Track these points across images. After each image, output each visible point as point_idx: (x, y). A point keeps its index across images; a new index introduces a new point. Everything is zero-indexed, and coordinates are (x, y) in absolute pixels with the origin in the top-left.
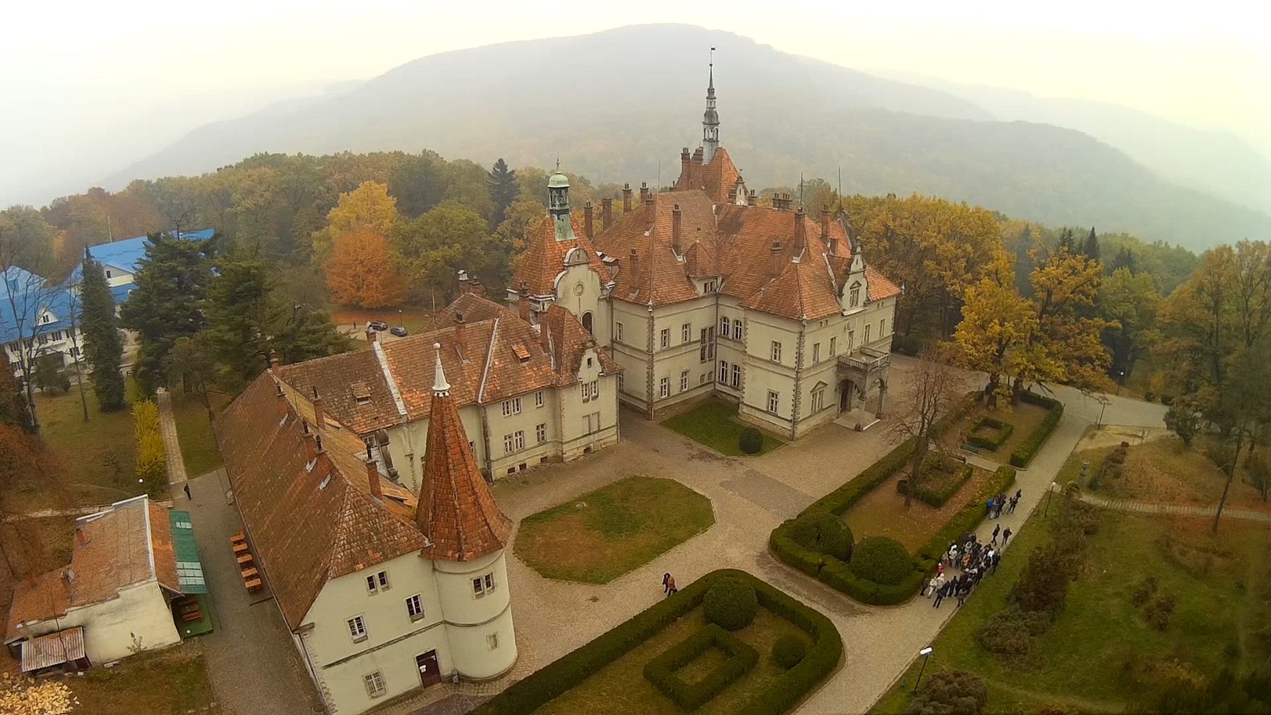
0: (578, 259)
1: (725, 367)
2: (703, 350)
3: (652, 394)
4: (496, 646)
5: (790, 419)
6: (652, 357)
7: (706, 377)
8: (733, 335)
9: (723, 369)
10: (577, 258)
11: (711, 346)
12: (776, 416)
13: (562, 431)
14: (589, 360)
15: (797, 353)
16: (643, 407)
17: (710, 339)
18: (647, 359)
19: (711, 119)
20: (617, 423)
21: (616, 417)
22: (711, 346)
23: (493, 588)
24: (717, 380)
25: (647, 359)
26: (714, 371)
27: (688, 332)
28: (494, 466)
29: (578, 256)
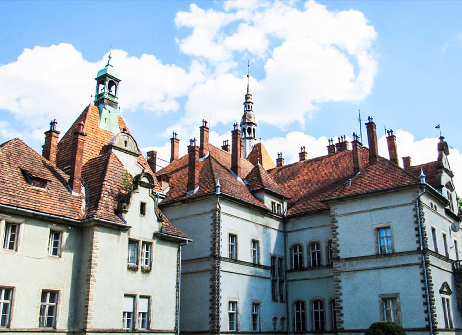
1: (301, 311)
2: (274, 281)
3: (218, 319)
5: (424, 326)
6: (219, 262)
7: (278, 321)
8: (309, 262)
9: (298, 314)
11: (281, 282)
13: (87, 306)
14: (143, 205)
15: (417, 229)
18: (211, 267)
20: (176, 329)
21: (174, 317)
22: (281, 282)
24: (291, 330)
25: (210, 268)
26: (286, 317)
27: (257, 252)
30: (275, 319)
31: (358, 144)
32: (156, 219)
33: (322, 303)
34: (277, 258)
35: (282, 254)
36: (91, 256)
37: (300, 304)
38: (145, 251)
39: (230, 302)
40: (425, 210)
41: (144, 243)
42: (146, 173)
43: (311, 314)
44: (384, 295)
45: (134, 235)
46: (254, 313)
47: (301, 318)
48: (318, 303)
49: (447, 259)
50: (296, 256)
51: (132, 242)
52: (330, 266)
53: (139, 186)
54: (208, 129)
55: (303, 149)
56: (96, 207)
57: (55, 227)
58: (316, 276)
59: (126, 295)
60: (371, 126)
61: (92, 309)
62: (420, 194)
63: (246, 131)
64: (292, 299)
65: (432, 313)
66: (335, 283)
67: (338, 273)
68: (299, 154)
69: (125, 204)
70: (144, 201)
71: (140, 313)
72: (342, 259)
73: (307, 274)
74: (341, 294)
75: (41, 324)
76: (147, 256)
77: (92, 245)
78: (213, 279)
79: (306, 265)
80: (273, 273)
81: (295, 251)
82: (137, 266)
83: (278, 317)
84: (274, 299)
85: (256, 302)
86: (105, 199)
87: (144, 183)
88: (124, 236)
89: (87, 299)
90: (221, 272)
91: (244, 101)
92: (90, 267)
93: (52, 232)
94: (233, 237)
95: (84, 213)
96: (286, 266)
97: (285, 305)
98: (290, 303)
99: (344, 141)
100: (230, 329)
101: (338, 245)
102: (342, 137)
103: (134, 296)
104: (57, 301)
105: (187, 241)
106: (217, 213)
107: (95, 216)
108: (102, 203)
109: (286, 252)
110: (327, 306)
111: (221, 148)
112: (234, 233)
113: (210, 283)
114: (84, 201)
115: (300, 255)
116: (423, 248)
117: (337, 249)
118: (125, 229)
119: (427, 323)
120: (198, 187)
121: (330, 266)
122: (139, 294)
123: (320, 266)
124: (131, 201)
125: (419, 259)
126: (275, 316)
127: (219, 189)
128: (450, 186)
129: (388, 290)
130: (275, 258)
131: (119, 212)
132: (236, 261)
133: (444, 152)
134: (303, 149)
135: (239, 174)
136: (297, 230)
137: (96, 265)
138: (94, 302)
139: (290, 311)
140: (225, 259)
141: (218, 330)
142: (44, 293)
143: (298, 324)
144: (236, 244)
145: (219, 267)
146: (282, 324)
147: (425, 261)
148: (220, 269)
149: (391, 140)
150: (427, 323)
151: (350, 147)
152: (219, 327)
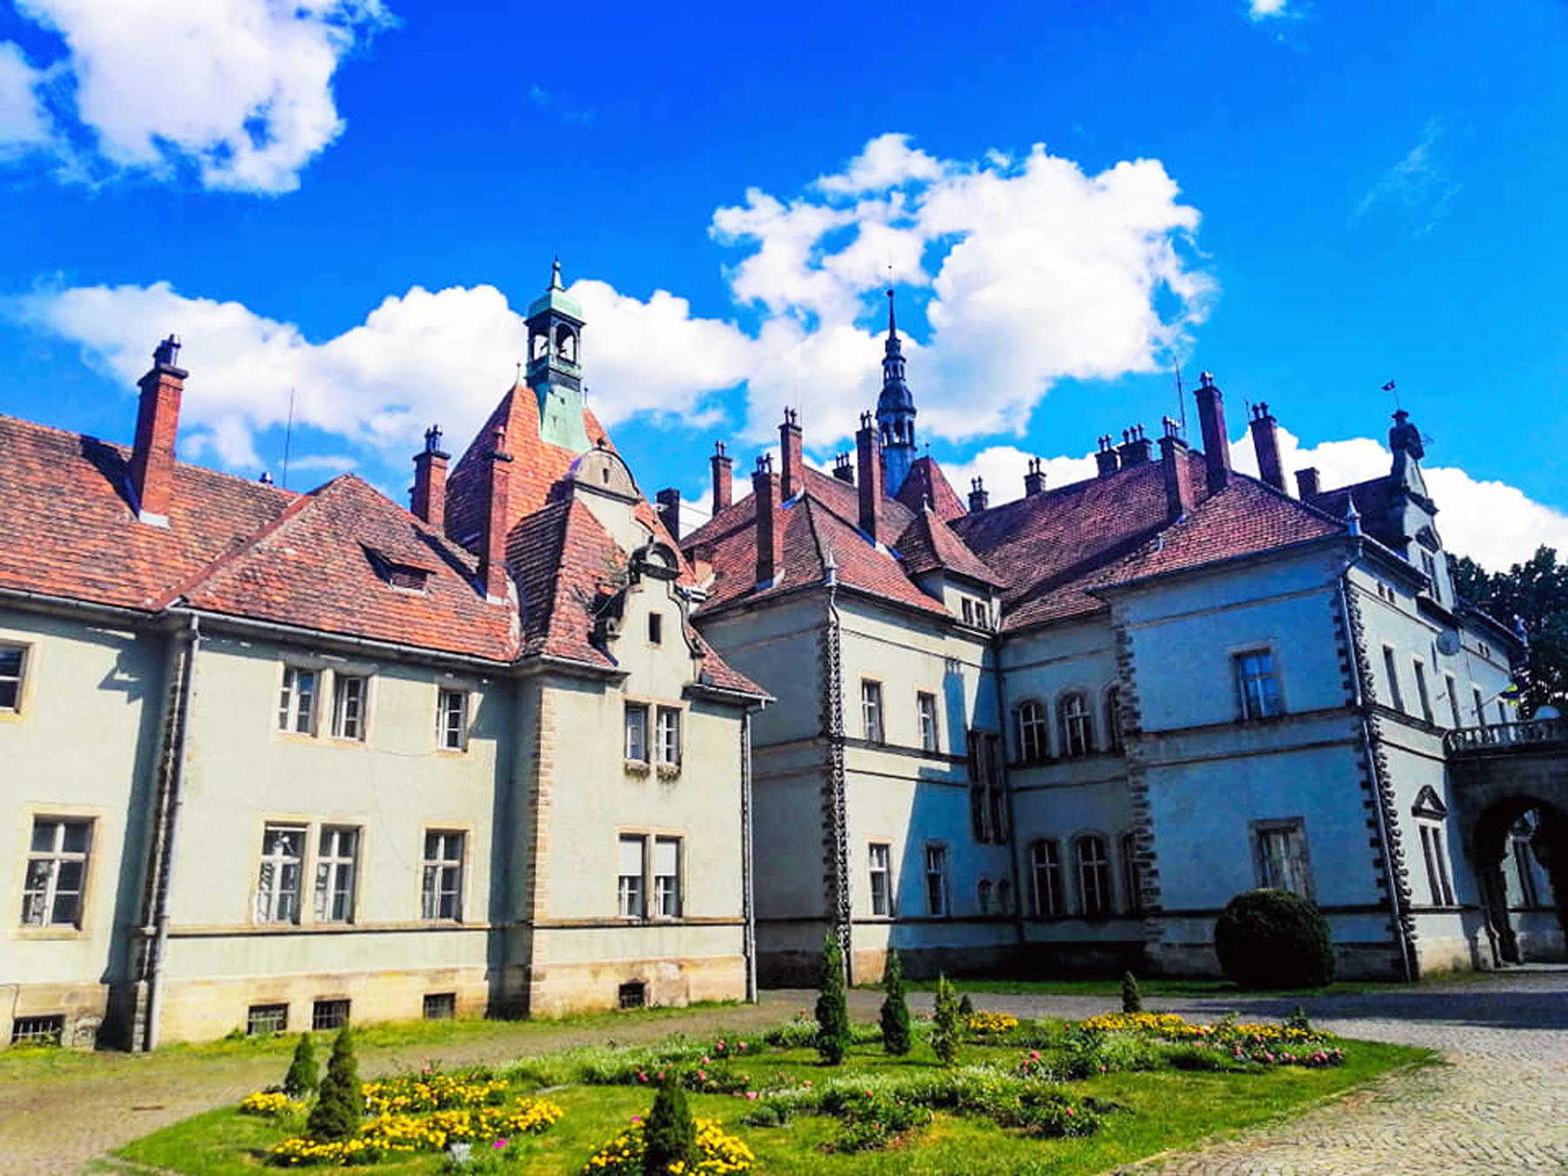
0: (606, 481)
1: (1048, 864)
2: (976, 793)
5: (1375, 900)
7: (993, 890)
8: (1063, 743)
9: (1042, 872)
10: (602, 477)
11: (995, 795)
14: (655, 621)
24: (1026, 910)
26: (1011, 879)
28: (172, 960)
29: (605, 471)
30: (985, 884)
31: (1177, 445)
32: (688, 651)
33: (1100, 845)
34: (982, 737)
36: (538, 746)
37: (1045, 847)
38: (664, 729)
39: (872, 846)
40: (1363, 603)
41: (661, 709)
42: (658, 545)
43: (1076, 870)
44: (1262, 822)
45: (636, 690)
46: (933, 871)
48: (1088, 845)
49: (1428, 726)
50: (1029, 729)
51: (635, 710)
52: (1116, 751)
53: (642, 575)
54: (800, 430)
55: (1035, 466)
56: (544, 629)
57: (450, 681)
58: (1082, 778)
59: (625, 837)
60: (1207, 398)
61: (544, 871)
62: (1347, 563)
63: (892, 429)
64: (1023, 835)
65: (1395, 867)
66: (1133, 795)
67: (1140, 769)
68: (1026, 477)
69: (612, 620)
70: (656, 611)
71: (658, 878)
72: (1148, 734)
73: (1060, 773)
74: (1149, 821)
75: (428, 912)
76: (668, 742)
77: (539, 720)
78: (828, 791)
79: (1055, 751)
80: (974, 774)
82: (645, 765)
83: (990, 879)
84: (980, 837)
85: (935, 845)
86: (564, 609)
87: (655, 568)
88: (614, 698)
89: (534, 849)
90: (846, 774)
91: (884, 355)
92: (537, 773)
93: (443, 692)
94: (871, 688)
95: (516, 645)
96: (1004, 754)
97: (1004, 850)
98: (1021, 845)
99: (1138, 438)
100: (876, 912)
101: (1136, 700)
102: (1133, 431)
103: (642, 839)
104: (463, 853)
105: (763, 703)
106: (831, 631)
107: (544, 650)
108: (558, 620)
109: (1002, 718)
110: (1114, 851)
111: (831, 475)
112: (873, 677)
113: (820, 801)
114: (515, 616)
115: (1040, 726)
116: (1363, 701)
117: (1132, 708)
119: (1383, 893)
120: (783, 571)
121: (1116, 751)
122: (653, 832)
123: (1092, 752)
124: (625, 612)
125: (1353, 729)
126: (982, 878)
127: (833, 573)
128: (1428, 538)
129: (1274, 809)
130: (978, 734)
131: (599, 639)
132: (881, 746)
133: (1410, 453)
134: (1035, 466)
135: (878, 536)
136: (1030, 666)
137: (550, 766)
138: (548, 854)
140: (855, 742)
141: (847, 915)
142: (432, 837)
143: (1043, 895)
144: (880, 705)
145: (841, 762)
146: (1002, 898)
147: (1371, 734)
148: (845, 767)
150: (1383, 893)
151: (1155, 453)
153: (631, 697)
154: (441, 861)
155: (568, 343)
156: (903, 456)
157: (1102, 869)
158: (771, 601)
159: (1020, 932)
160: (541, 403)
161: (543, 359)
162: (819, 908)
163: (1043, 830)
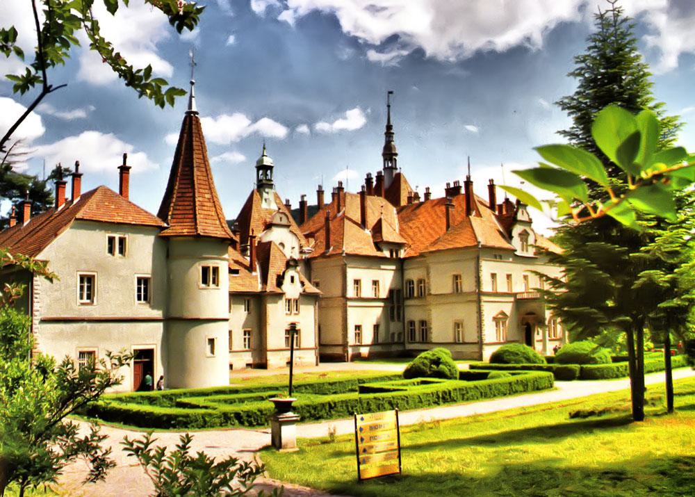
4: (212, 352)
5: (476, 341)
7: (396, 336)
8: (418, 293)
9: (411, 330)
11: (399, 308)
12: (464, 343)
16: (339, 351)
17: (398, 301)
19: (389, 154)
22: (399, 308)
23: (218, 285)
29: (281, 218)
35: (399, 287)
37: (412, 323)
45: (288, 296)
47: (412, 332)
48: (423, 323)
79: (416, 295)
81: (410, 284)
94: (357, 282)
97: (400, 324)
112: (357, 278)
118: (281, 295)
139: (406, 328)
140: (351, 299)
149: (492, 188)
151: (463, 191)
152: (347, 342)
153: (287, 297)
154: (247, 336)
155: (269, 172)
156: (392, 172)
157: (426, 330)
158: (329, 257)
159: (405, 347)
160: (261, 196)
161: (261, 180)
162: (341, 343)
163: (412, 318)
